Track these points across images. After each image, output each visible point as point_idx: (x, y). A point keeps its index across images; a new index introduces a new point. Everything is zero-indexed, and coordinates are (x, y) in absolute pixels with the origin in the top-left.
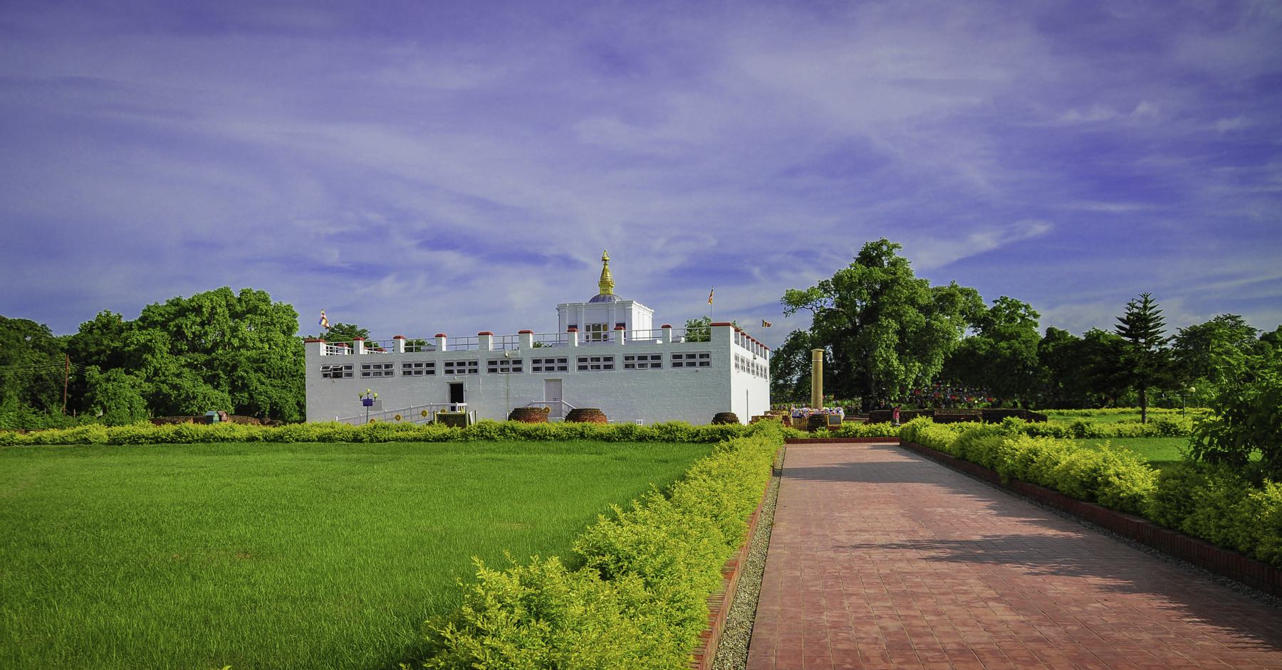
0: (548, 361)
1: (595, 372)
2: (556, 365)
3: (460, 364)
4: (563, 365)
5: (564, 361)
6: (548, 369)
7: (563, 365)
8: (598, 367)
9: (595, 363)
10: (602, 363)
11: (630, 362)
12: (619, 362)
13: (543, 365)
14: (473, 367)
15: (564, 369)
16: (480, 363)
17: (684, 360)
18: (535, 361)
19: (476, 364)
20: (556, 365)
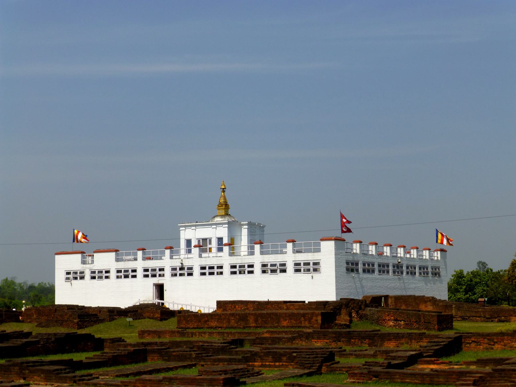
6: (154, 276)
10: (185, 272)
12: (197, 271)
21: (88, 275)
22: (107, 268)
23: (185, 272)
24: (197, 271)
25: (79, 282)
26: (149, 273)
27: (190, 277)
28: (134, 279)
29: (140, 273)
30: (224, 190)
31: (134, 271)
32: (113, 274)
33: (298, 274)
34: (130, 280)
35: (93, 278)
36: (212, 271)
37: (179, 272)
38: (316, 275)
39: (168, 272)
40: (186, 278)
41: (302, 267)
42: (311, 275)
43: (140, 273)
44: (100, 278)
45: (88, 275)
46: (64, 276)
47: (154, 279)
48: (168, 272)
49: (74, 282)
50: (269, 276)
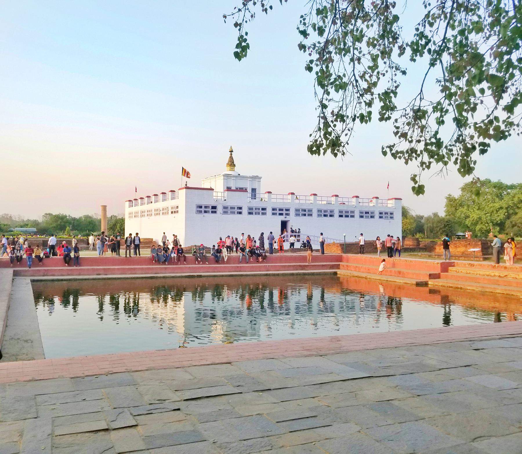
0: (280, 210)
2: (284, 212)
3: (232, 208)
4: (287, 212)
5: (287, 210)
7: (287, 212)
8: (305, 215)
9: (304, 213)
11: (320, 213)
13: (278, 212)
14: (240, 211)
15: (287, 214)
16: (243, 208)
18: (273, 210)
19: (240, 208)
20: (284, 212)
21: (220, 209)
22: (240, 205)
24: (315, 213)
25: (210, 216)
28: (264, 216)
30: (231, 151)
31: (263, 209)
32: (245, 211)
35: (225, 213)
36: (326, 214)
38: (391, 220)
39: (292, 212)
41: (384, 215)
43: (269, 211)
46: (195, 209)
47: (282, 216)
49: (206, 214)
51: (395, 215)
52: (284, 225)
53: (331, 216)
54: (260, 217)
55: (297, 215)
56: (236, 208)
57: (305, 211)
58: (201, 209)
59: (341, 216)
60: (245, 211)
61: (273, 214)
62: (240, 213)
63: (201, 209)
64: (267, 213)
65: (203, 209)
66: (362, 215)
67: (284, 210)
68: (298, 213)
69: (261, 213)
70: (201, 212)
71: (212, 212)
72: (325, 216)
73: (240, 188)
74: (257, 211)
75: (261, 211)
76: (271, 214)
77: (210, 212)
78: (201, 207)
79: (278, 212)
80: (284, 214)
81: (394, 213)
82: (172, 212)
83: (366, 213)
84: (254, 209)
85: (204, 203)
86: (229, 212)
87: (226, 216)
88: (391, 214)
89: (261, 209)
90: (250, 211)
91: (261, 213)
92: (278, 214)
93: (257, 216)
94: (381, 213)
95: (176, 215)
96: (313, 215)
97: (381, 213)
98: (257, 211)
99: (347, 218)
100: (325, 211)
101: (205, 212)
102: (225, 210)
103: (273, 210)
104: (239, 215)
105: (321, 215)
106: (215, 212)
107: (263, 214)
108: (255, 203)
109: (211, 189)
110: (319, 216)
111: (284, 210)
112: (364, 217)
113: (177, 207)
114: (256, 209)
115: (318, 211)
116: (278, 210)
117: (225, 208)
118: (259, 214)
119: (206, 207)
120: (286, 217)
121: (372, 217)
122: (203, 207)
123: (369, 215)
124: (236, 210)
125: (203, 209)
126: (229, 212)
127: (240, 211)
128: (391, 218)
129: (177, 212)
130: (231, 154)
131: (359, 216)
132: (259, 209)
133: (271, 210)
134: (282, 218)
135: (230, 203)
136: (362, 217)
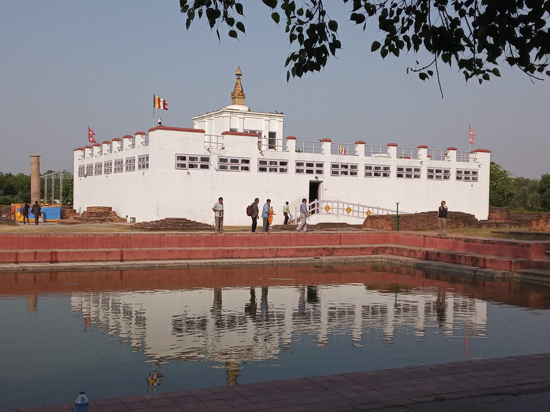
1: (344, 177)
2: (315, 168)
3: (233, 161)
4: (319, 169)
5: (320, 165)
7: (319, 169)
8: (346, 173)
9: (344, 170)
12: (361, 171)
13: (305, 168)
14: (245, 165)
15: (319, 172)
17: (404, 173)
18: (298, 164)
19: (247, 162)
20: (315, 168)
21: (214, 162)
22: (246, 156)
23: (349, 170)
24: (361, 171)
26: (300, 167)
27: (353, 177)
28: (283, 175)
29: (291, 167)
31: (283, 163)
32: (254, 165)
33: (459, 182)
34: (278, 174)
35: (223, 168)
37: (340, 169)
38: (474, 183)
39: (327, 169)
40: (349, 177)
42: (469, 184)
43: (291, 167)
44: (235, 168)
45: (214, 162)
46: (173, 161)
48: (327, 169)
49: (191, 170)
50: (434, 182)
51: (480, 176)
52: (314, 188)
53: (385, 175)
54: (277, 175)
55: (335, 173)
56: (240, 161)
57: (346, 167)
58: (185, 162)
59: (399, 176)
60: (254, 165)
61: (298, 171)
62: (247, 169)
63: (185, 162)
64: (289, 170)
65: (187, 162)
66: (431, 174)
67: (315, 165)
68: (335, 169)
69: (278, 170)
70: (183, 166)
71: (203, 167)
72: (376, 175)
73: (251, 131)
74: (273, 166)
75: (279, 167)
76: (294, 171)
77: (199, 166)
78: (184, 158)
79: (305, 168)
80: (315, 172)
81: (479, 173)
82: (140, 166)
83: (437, 171)
84: (268, 163)
85: (189, 152)
86: (229, 167)
87: (223, 173)
88: (475, 173)
89: (278, 163)
90: (263, 166)
91: (278, 170)
92: (305, 171)
93: (273, 174)
94: (459, 172)
95: (145, 170)
96: (359, 173)
97: (459, 172)
98: (273, 166)
99: (409, 180)
100: (377, 168)
101: (191, 166)
102: (223, 164)
103: (298, 164)
104: (245, 172)
105: (370, 174)
106: (206, 167)
107: (282, 170)
108: (269, 155)
109: (203, 131)
110: (368, 175)
111: (315, 165)
112: (435, 177)
113: (147, 158)
114: (271, 163)
115: (367, 168)
116: (305, 165)
117: (223, 160)
118: (276, 170)
119: (192, 159)
120: (316, 177)
121: (445, 178)
122: (187, 158)
123: (442, 174)
124: (241, 165)
125: (187, 162)
126: (229, 167)
127: (245, 165)
128: (475, 179)
129: (148, 165)
130: (239, 78)
131: (426, 177)
132: (276, 163)
133: (295, 164)
134: (312, 177)
135: (229, 154)
136: (430, 177)
